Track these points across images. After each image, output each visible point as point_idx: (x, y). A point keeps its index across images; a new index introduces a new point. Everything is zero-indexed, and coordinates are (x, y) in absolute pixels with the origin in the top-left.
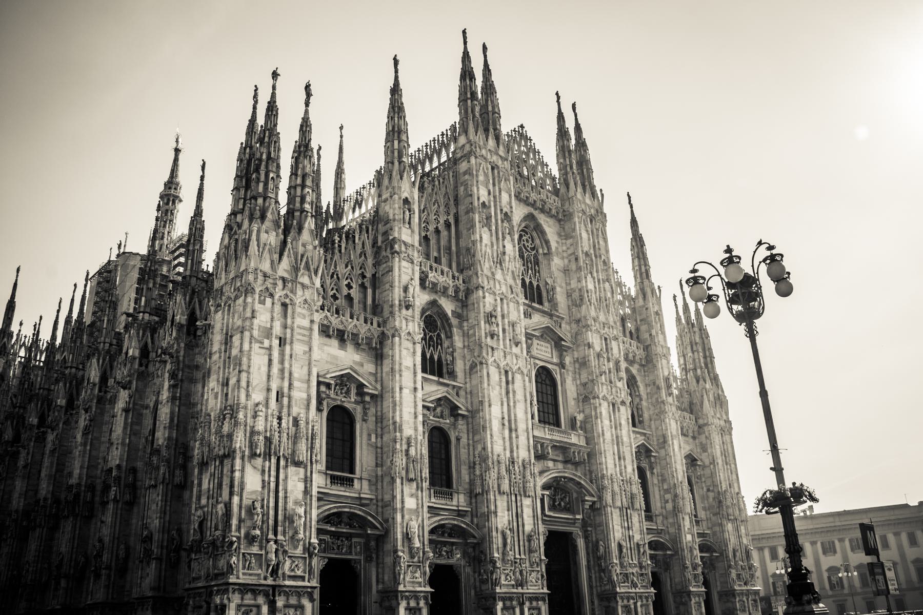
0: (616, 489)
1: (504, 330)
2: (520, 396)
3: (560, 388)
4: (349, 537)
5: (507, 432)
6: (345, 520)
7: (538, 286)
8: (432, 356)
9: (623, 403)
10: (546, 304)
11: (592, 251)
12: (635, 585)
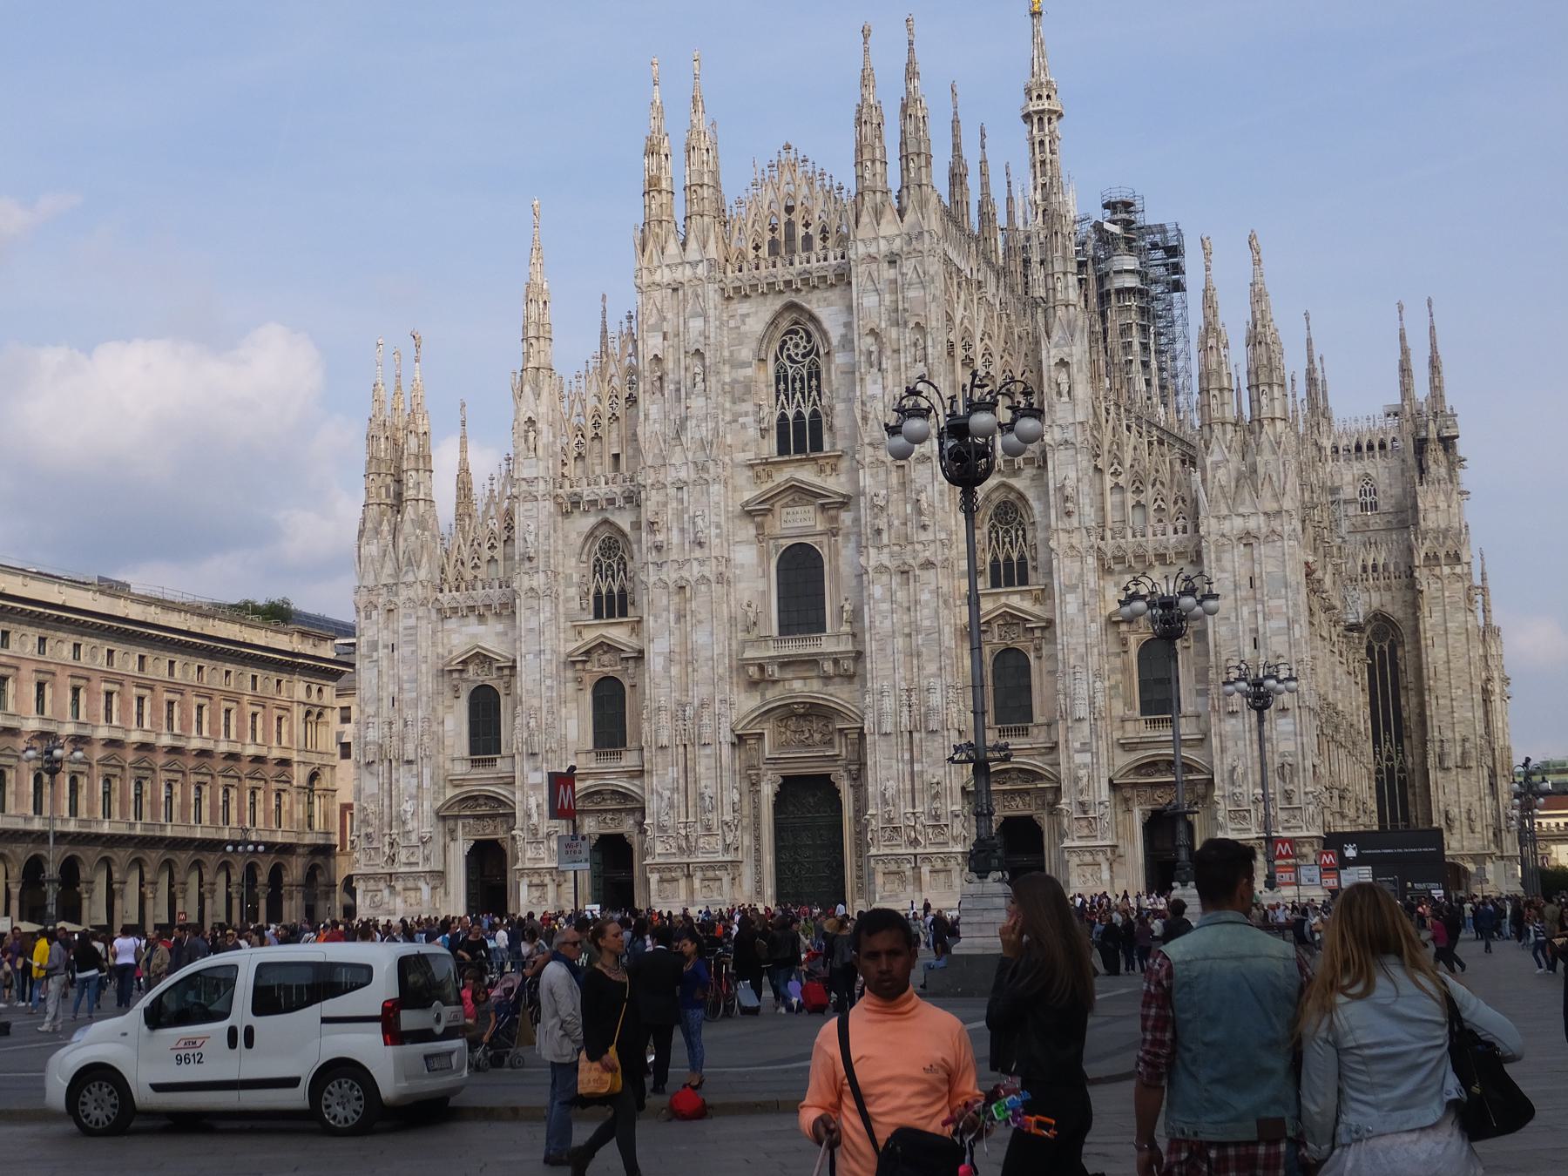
0: (888, 704)
1: (682, 530)
2: (704, 615)
3: (826, 568)
4: (491, 817)
5: (674, 671)
6: (481, 801)
7: (815, 414)
8: (610, 591)
9: (928, 565)
10: (826, 437)
11: (883, 325)
12: (915, 842)
